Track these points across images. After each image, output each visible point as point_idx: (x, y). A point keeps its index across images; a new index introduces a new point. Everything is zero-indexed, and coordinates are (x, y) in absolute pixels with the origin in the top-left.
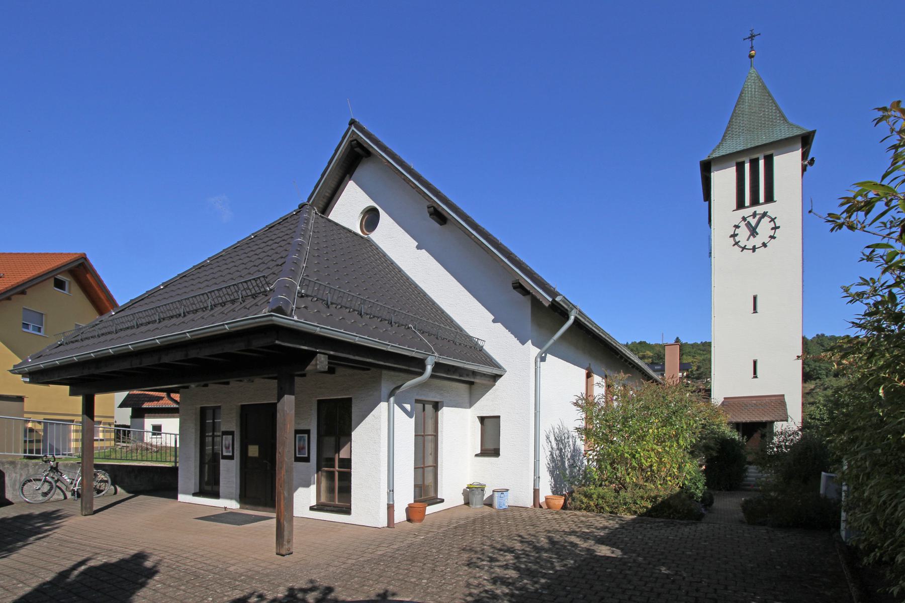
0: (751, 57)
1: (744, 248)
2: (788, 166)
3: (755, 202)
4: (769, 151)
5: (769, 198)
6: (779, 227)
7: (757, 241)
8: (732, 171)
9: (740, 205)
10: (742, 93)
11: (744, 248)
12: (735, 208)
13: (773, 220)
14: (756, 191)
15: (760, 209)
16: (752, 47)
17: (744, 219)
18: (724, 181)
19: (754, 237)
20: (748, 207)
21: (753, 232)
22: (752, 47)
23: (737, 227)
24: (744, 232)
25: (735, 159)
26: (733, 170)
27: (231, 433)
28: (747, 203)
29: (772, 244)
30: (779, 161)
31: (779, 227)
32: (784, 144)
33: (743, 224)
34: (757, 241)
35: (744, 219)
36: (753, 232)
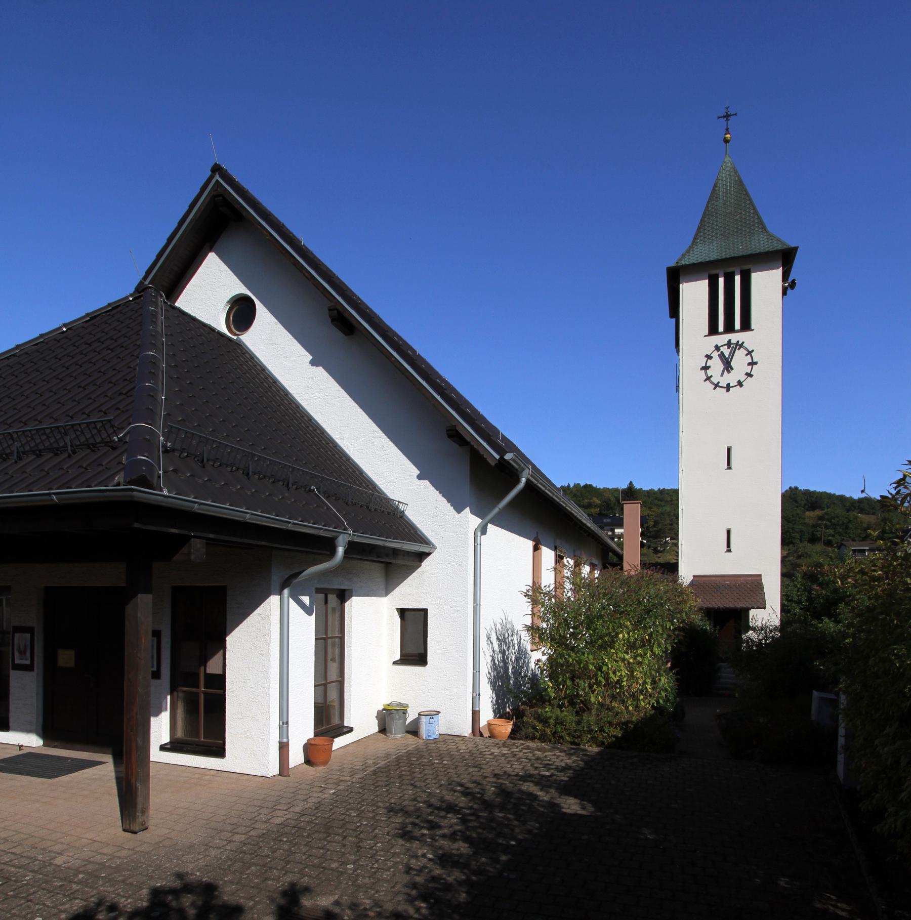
0: (726, 141)
1: (717, 385)
2: (766, 284)
3: (730, 328)
4: (746, 264)
5: (746, 325)
6: (756, 363)
7: (731, 378)
8: (702, 286)
9: (713, 330)
10: (715, 186)
11: (717, 385)
12: (707, 333)
13: (750, 353)
14: (732, 315)
15: (734, 337)
16: (727, 129)
17: (717, 348)
18: (695, 294)
19: (729, 372)
20: (721, 333)
21: (728, 366)
22: (727, 129)
23: (709, 357)
24: (716, 365)
26: (705, 283)
27: (30, 630)
28: (721, 328)
31: (756, 363)
32: (764, 260)
33: (715, 355)
34: (731, 378)
35: (717, 348)
36: (728, 366)
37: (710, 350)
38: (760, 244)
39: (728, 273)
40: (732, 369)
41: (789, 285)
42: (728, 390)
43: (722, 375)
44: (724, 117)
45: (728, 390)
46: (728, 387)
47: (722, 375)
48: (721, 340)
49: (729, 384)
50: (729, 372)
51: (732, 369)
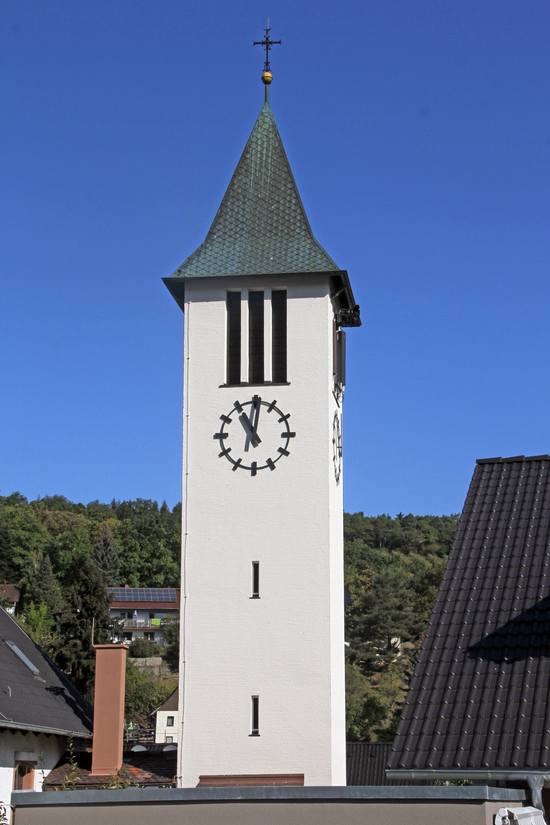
0: (266, 82)
1: (237, 464)
2: (311, 318)
3: (257, 378)
4: (281, 288)
5: (280, 378)
6: (293, 435)
7: (259, 455)
8: (219, 309)
9: (234, 379)
10: (246, 151)
11: (237, 464)
13: (284, 418)
14: (258, 360)
15: (267, 393)
16: (267, 64)
17: (238, 406)
18: (206, 323)
19: (255, 445)
20: (245, 385)
22: (267, 64)
23: (226, 419)
24: (237, 433)
25: (230, 289)
28: (245, 376)
29: (282, 463)
30: (294, 306)
31: (293, 435)
32: (307, 282)
33: (235, 416)
34: (259, 455)
35: (238, 406)
37: (227, 408)
38: (302, 260)
39: (258, 298)
40: (259, 441)
41: (347, 314)
42: (254, 473)
43: (247, 449)
44: (263, 43)
45: (254, 473)
46: (254, 469)
47: (247, 449)
48: (245, 394)
49: (254, 464)
50: (255, 445)
51: (259, 441)
